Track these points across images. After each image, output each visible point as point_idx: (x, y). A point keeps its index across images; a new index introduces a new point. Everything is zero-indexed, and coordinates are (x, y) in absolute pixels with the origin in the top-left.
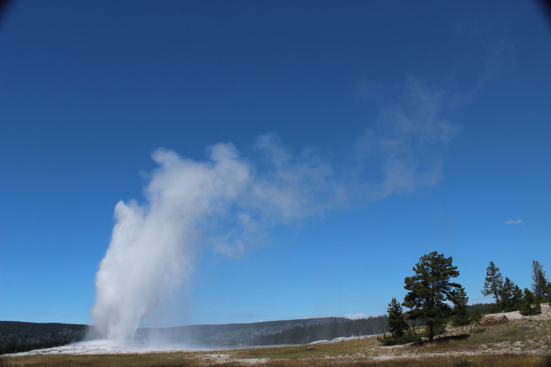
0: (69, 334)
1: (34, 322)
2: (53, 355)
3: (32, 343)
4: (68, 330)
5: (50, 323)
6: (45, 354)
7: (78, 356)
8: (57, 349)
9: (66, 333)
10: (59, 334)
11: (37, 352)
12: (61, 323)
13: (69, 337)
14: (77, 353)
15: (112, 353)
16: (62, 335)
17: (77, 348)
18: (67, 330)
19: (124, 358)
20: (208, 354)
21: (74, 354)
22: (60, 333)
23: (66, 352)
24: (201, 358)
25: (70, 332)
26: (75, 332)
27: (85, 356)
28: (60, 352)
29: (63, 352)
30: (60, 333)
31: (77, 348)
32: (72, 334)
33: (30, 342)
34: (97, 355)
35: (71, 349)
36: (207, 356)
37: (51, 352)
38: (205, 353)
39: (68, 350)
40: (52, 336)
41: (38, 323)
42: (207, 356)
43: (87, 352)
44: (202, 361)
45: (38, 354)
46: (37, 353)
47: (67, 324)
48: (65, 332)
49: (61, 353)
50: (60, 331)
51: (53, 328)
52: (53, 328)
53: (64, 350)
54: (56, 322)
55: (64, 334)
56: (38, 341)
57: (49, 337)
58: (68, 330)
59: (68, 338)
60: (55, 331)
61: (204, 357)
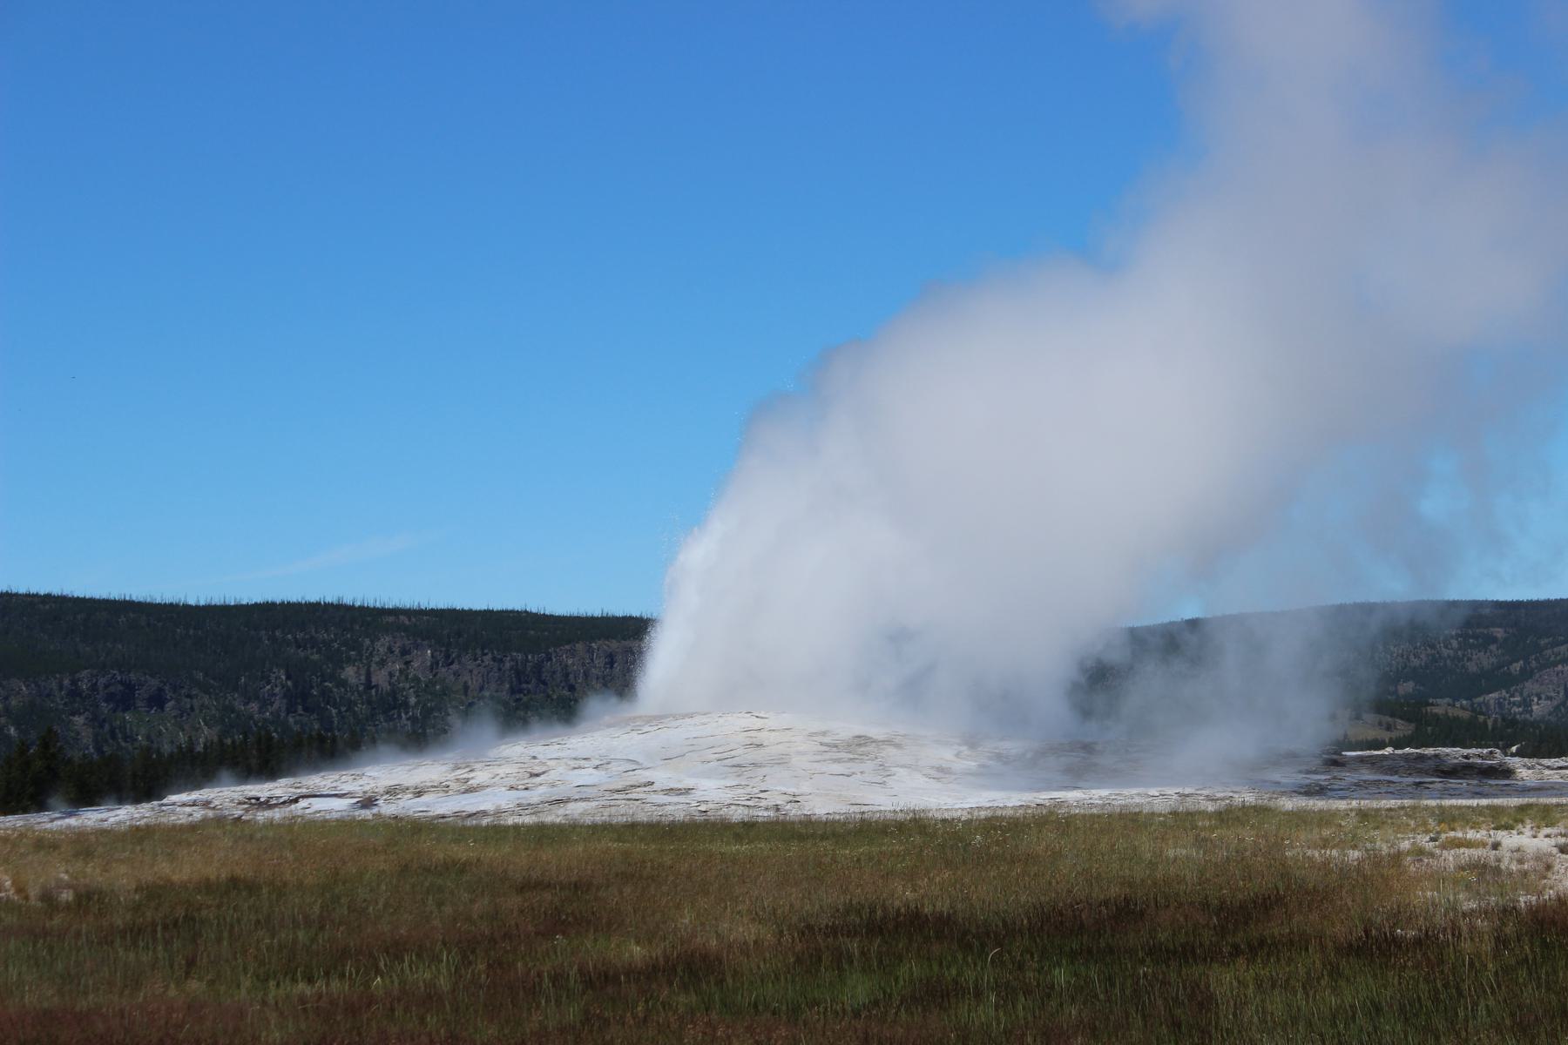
0: (416, 679)
1: (158, 600)
2: (322, 827)
3: (167, 748)
4: (404, 652)
5: (273, 604)
6: (262, 816)
7: (496, 833)
8: (346, 788)
9: (391, 675)
10: (343, 683)
11: (206, 804)
12: (348, 600)
13: (413, 700)
14: (484, 813)
15: (737, 815)
16: (369, 686)
17: (480, 776)
18: (397, 651)
19: (827, 845)
20: (1476, 826)
21: (469, 823)
22: (349, 673)
23: (407, 806)
24: (1419, 852)
25: (415, 664)
26: (455, 667)
27: (542, 834)
28: (368, 802)
29: (387, 808)
30: (349, 673)
31: (480, 776)
32: (434, 684)
33: (148, 738)
34: (633, 826)
35: (444, 788)
36: (1469, 844)
37: (303, 803)
38: (1449, 818)
39: (419, 793)
40: (298, 697)
41: (192, 602)
42: (1469, 844)
43: (551, 803)
44: (1438, 878)
45: (220, 821)
46: (210, 814)
47: (396, 612)
48: (382, 663)
49: (375, 810)
50: (349, 660)
51: (300, 636)
52: (300, 636)
53: (392, 791)
54: (313, 597)
55: (380, 678)
56: (206, 735)
57: (279, 704)
58: (404, 652)
59: (406, 705)
60: (316, 657)
61: (1443, 847)
